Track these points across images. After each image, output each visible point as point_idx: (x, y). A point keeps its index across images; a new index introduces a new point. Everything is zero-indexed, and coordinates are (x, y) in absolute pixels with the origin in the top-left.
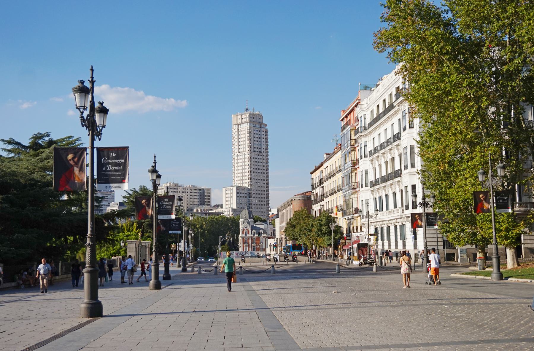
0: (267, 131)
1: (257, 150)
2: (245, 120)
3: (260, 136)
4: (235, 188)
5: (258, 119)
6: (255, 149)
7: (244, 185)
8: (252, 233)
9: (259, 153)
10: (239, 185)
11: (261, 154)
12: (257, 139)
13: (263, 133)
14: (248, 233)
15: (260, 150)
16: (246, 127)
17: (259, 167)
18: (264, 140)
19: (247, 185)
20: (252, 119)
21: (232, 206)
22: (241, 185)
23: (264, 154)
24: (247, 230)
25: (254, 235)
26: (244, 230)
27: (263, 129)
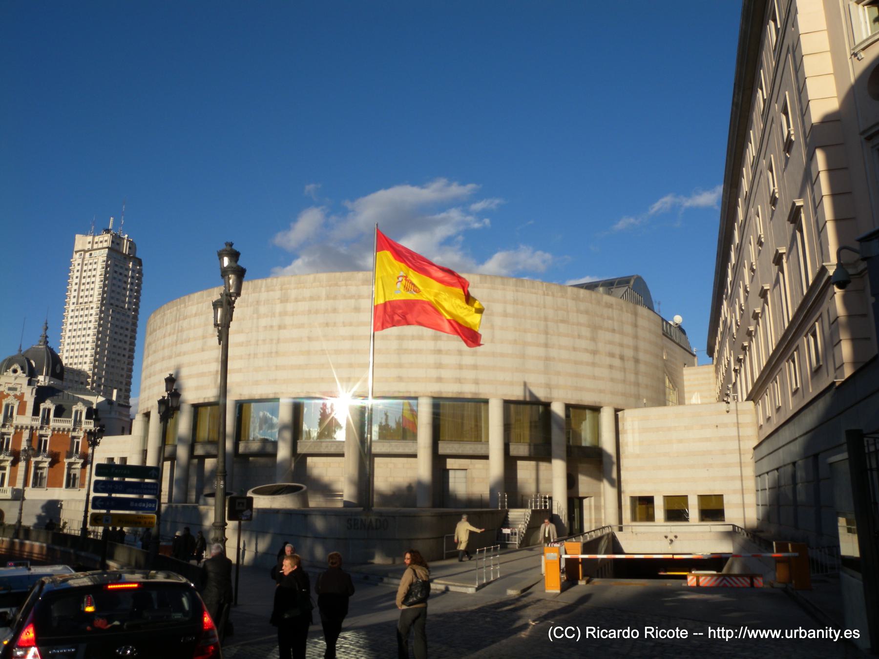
2: (100, 246)
8: (36, 412)
14: (22, 411)
16: (101, 256)
24: (20, 398)
25: (46, 421)
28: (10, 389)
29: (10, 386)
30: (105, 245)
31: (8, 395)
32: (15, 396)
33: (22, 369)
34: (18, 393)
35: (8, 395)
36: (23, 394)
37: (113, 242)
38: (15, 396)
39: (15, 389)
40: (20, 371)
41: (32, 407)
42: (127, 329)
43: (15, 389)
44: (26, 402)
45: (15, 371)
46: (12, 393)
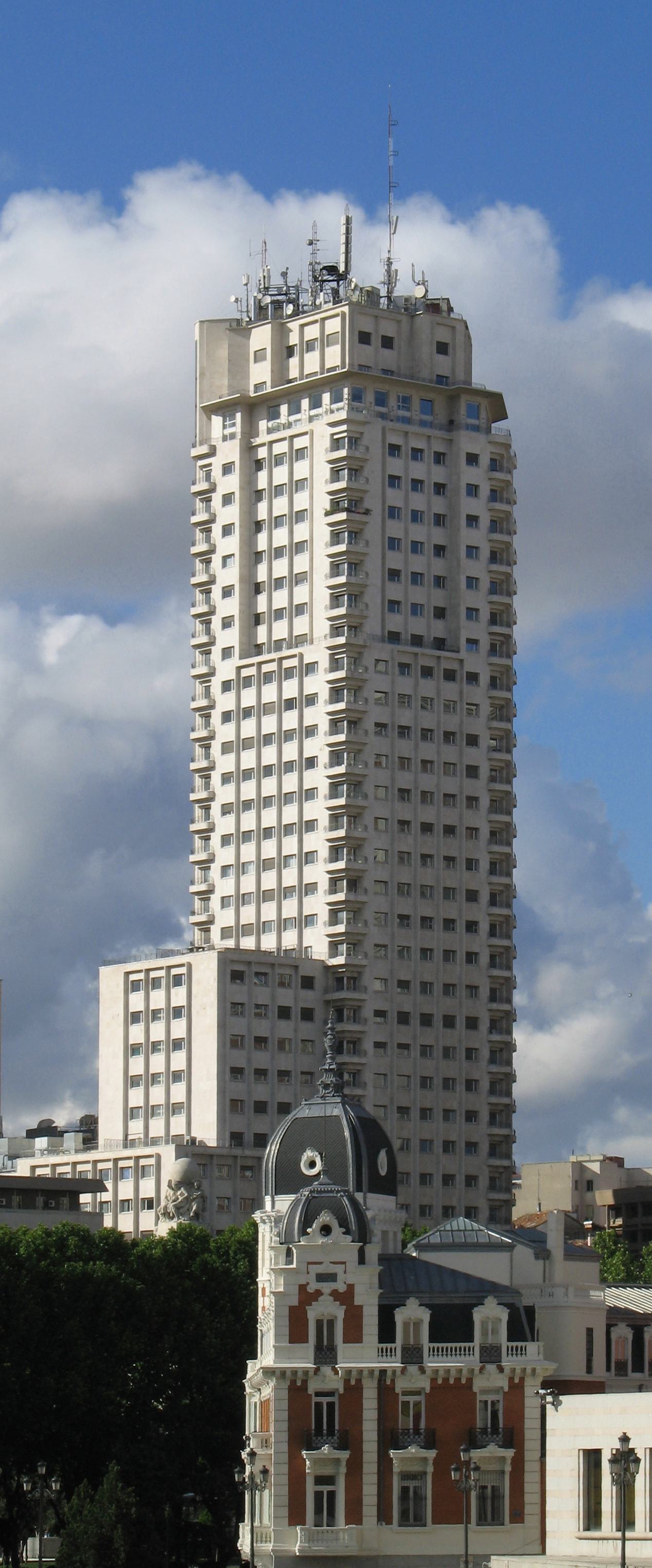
0: (502, 462)
1: (418, 626)
3: (439, 505)
4: (206, 971)
5: (426, 350)
6: (395, 622)
7: (290, 939)
8: (386, 1333)
9: (427, 656)
10: (248, 943)
11: (447, 660)
12: (418, 532)
13: (470, 475)
14: (354, 1334)
15: (438, 629)
17: (427, 782)
18: (479, 537)
19: (317, 943)
20: (371, 354)
21: (178, 1125)
22: (269, 942)
23: (478, 662)
24: (346, 1297)
26: (307, 1297)
27: (468, 442)
28: (321, 1278)
29: (320, 1269)
30: (334, 356)
31: (318, 1293)
32: (335, 1294)
33: (343, 1223)
34: (342, 1288)
35: (318, 1293)
36: (351, 1287)
37: (364, 338)
38: (335, 1294)
39: (332, 1277)
40: (337, 1230)
41: (375, 1320)
42: (473, 740)
43: (332, 1277)
44: (361, 1307)
45: (326, 1230)
46: (327, 1287)
